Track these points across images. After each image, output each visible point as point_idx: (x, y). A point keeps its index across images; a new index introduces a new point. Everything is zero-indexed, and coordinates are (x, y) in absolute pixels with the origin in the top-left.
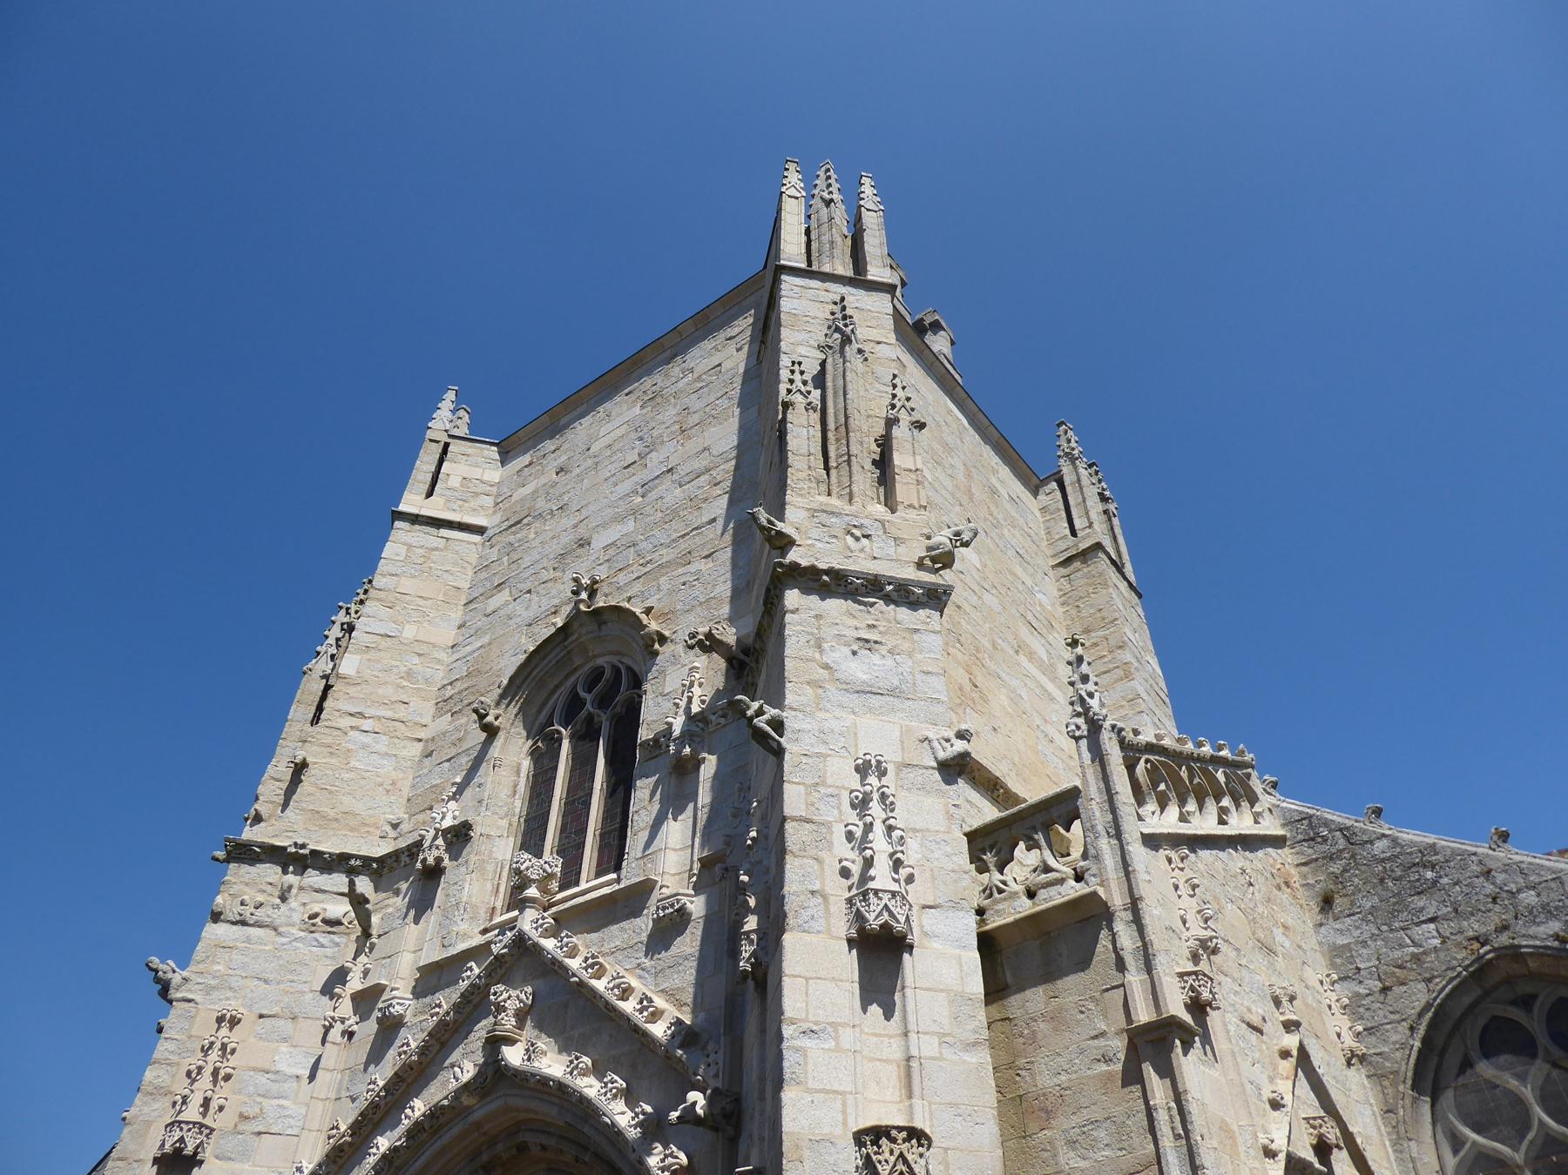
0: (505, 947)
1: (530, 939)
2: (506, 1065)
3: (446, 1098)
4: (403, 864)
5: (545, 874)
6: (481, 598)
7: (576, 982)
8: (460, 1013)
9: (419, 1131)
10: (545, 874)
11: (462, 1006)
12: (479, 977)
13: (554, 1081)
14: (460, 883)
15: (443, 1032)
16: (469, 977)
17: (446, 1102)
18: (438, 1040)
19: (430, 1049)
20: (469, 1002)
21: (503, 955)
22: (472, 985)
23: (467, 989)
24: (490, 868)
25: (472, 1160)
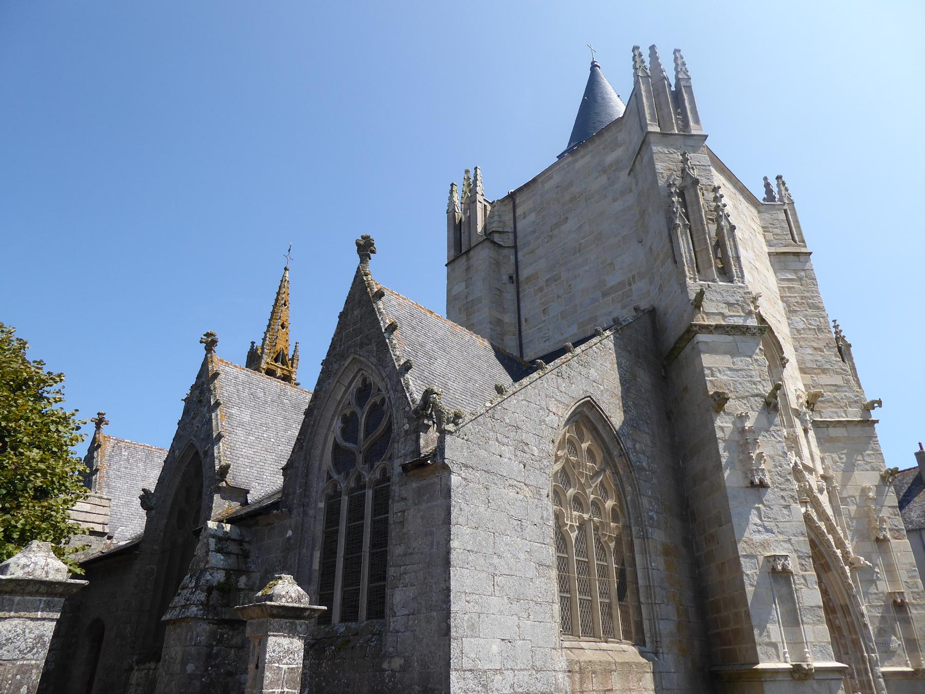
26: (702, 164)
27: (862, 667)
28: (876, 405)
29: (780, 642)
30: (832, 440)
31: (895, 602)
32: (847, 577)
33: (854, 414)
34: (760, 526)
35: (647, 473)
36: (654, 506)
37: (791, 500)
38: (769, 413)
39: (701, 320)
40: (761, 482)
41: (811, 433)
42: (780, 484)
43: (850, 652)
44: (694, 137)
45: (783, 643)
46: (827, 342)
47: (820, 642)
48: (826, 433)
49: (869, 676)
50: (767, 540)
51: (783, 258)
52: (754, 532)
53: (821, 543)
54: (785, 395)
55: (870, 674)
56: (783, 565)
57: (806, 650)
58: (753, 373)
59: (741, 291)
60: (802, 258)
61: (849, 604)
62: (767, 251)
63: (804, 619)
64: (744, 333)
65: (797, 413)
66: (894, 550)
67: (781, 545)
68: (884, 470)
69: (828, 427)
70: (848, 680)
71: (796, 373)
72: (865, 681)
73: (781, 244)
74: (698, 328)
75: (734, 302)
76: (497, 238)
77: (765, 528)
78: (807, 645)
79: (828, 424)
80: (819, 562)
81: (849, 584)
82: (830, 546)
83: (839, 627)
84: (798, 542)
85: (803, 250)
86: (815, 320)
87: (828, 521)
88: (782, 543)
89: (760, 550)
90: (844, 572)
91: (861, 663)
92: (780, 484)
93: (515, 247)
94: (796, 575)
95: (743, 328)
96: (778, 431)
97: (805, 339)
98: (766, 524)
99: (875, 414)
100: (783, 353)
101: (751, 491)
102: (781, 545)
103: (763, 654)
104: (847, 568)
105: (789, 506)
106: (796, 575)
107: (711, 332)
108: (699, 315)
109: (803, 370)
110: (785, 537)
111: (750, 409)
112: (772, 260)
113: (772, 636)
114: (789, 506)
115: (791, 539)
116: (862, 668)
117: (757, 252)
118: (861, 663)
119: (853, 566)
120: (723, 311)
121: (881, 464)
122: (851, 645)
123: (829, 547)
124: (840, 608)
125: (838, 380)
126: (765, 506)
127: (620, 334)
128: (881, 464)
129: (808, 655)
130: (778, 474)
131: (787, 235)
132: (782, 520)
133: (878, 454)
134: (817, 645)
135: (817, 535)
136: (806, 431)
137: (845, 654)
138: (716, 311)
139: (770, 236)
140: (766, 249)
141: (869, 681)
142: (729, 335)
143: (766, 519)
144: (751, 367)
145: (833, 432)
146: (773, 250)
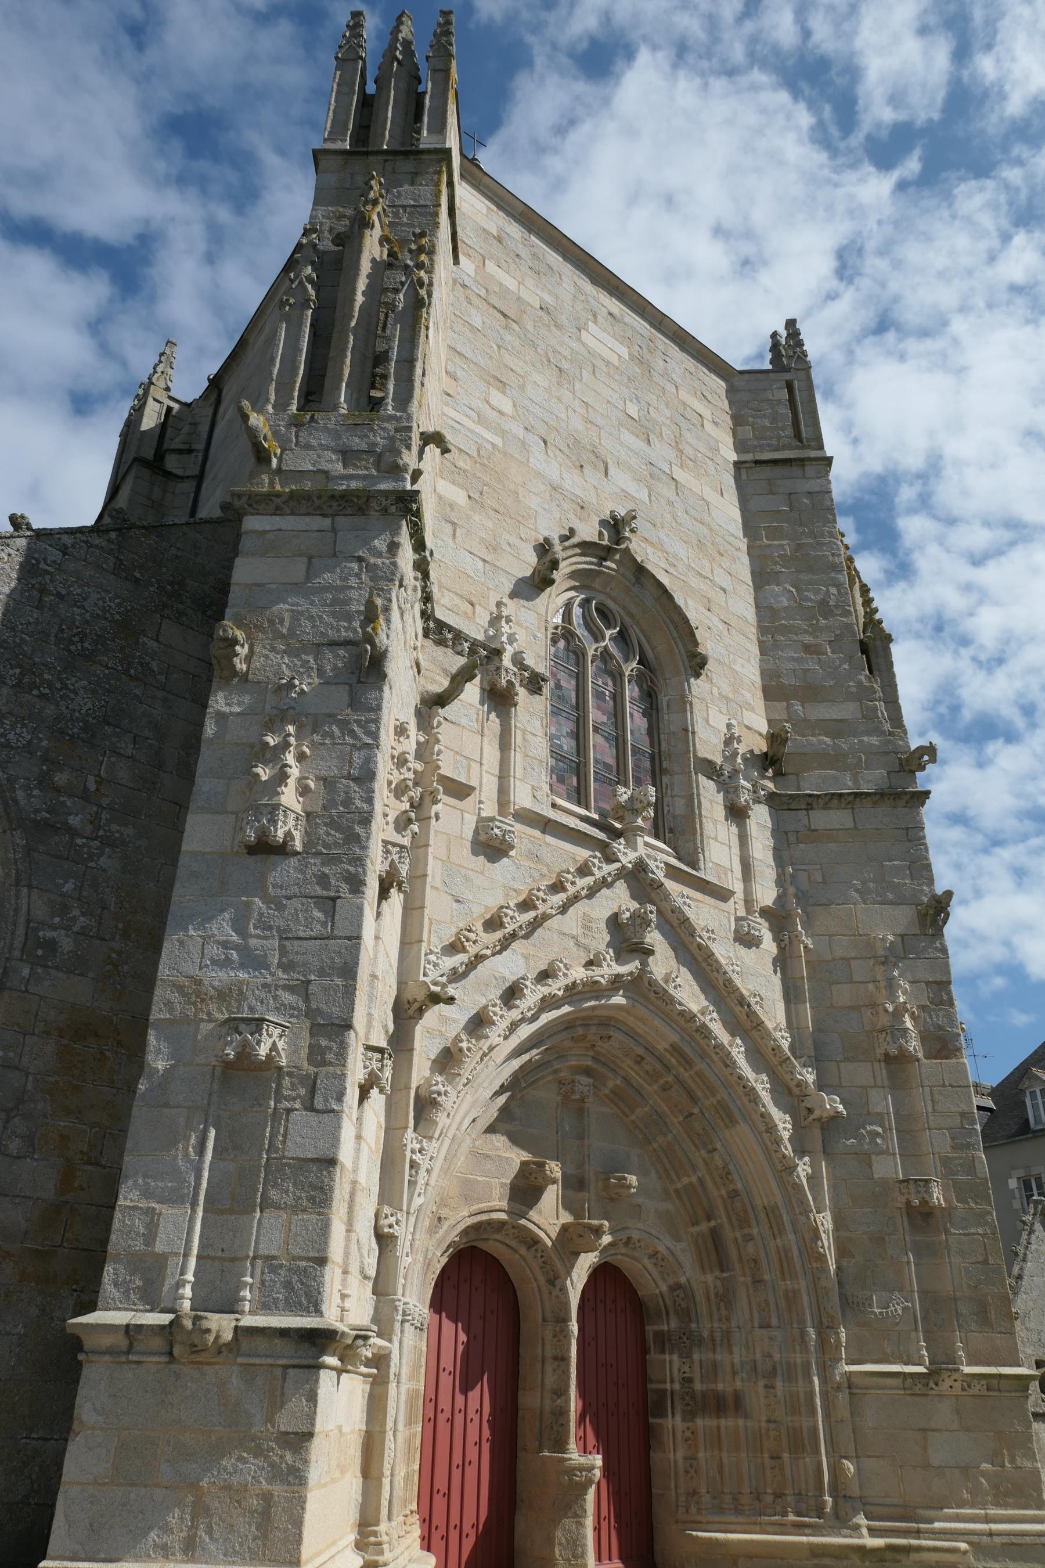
4: (459, 648)
6: (472, 366)
25: (566, 1028)
26: (422, 202)
27: (799, 1359)
28: (926, 758)
29: (177, 1254)
30: (813, 835)
31: (908, 1203)
32: (778, 1141)
33: (871, 780)
34: (236, 947)
35: (79, 841)
36: (74, 919)
37: (344, 887)
38: (359, 682)
39: (264, 483)
40: (263, 836)
41: (760, 817)
42: (326, 846)
43: (774, 1321)
44: (425, 157)
45: (186, 1255)
46: (838, 632)
47: (296, 1258)
48: (805, 821)
49: (812, 1382)
50: (241, 982)
51: (767, 472)
52: (214, 962)
53: (703, 1056)
54: (686, 730)
55: (816, 1379)
56: (245, 1044)
57: (249, 1280)
58: (354, 594)
59: (390, 426)
60: (810, 470)
61: (780, 1203)
62: (733, 457)
63: (274, 1194)
64: (362, 511)
65: (710, 769)
66: (926, 1083)
67: (275, 998)
68: (925, 900)
69: (809, 807)
70: (761, 1390)
71: (748, 695)
72: (802, 1395)
73: (769, 445)
74: (244, 499)
75: (365, 447)
76: (172, 463)
77: (244, 950)
78: (253, 1265)
79: (810, 802)
80: (707, 1103)
81: (784, 1156)
82: (728, 1062)
83: (755, 1261)
84: (326, 990)
85: (813, 454)
86: (817, 592)
87: (743, 1007)
88: (280, 992)
89: (213, 1007)
90: (771, 1128)
91: (797, 1348)
92: (326, 846)
93: (200, 478)
94: (290, 1074)
95: (359, 497)
96: (368, 721)
97: (785, 630)
98: (253, 942)
99: (922, 780)
100: (696, 644)
101: (250, 860)
102: (275, 998)
103: (116, 1285)
104: (783, 1123)
105: (334, 899)
106: (290, 1074)
107: (278, 511)
108: (265, 478)
109: (772, 691)
110: (295, 976)
111: (314, 674)
112: (744, 476)
113: (161, 1235)
114: (334, 899)
115: (309, 982)
116: (799, 1361)
117: (689, 451)
118: (797, 1348)
119: (812, 1117)
120: (324, 466)
121: (925, 888)
122: (783, 1304)
123: (727, 1066)
124: (762, 1215)
125: (847, 711)
126: (267, 899)
127: (109, 541)
128: (925, 888)
129: (246, 1293)
130: (333, 820)
131: (783, 429)
132: (301, 934)
133: (922, 869)
134: (281, 1266)
135: (691, 1036)
136: (737, 813)
137: (761, 1327)
138: (312, 468)
139: (747, 432)
140: (733, 457)
141: (811, 1394)
142: (324, 515)
143: (258, 932)
144: (353, 582)
145: (821, 819)
146: (749, 457)
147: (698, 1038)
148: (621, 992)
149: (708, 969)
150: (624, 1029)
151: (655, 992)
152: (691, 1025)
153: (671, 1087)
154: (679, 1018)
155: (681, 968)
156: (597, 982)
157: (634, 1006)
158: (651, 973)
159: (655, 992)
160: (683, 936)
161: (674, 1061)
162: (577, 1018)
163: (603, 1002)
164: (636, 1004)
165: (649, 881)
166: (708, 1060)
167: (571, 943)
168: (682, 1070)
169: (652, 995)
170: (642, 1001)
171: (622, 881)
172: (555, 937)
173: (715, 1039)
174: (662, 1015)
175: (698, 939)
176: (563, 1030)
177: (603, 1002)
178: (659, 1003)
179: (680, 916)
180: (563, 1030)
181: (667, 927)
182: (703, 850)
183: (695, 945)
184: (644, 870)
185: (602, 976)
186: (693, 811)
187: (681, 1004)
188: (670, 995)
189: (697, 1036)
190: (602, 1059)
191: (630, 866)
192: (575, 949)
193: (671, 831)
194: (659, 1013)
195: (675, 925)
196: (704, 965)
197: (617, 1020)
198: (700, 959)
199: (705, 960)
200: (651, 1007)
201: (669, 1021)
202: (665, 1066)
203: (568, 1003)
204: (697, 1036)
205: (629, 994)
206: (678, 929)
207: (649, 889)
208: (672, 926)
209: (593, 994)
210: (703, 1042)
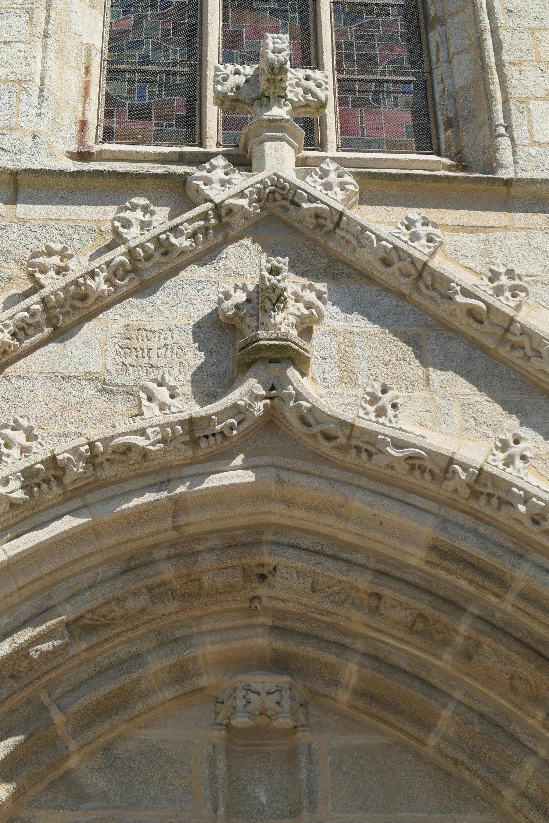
0: (241, 194)
1: (312, 199)
2: (312, 409)
3: (142, 432)
5: (309, 97)
7: (471, 312)
8: (112, 285)
9: (47, 481)
10: (309, 97)
11: (120, 273)
12: (174, 230)
13: (465, 468)
14: (23, 46)
15: (67, 308)
16: (144, 225)
17: (140, 441)
18: (51, 321)
19: (31, 331)
20: (135, 271)
21: (230, 211)
22: (156, 239)
23: (142, 246)
24: (71, 44)
147: (487, 510)
148: (238, 460)
149: (515, 356)
150: (306, 544)
151: (328, 437)
152: (450, 485)
153: (479, 645)
154: (416, 479)
155: (434, 373)
156: (129, 448)
157: (280, 482)
158: (299, 396)
159: (328, 437)
160: (431, 306)
161: (463, 583)
162: (155, 546)
163: (182, 489)
164: (285, 476)
165: (311, 222)
166: (536, 557)
167: (90, 390)
168: (493, 599)
169: (325, 446)
170: (306, 466)
171: (247, 241)
172: (41, 390)
173: (526, 499)
174: (373, 486)
175: (460, 299)
176: (114, 578)
177: (182, 489)
178: (351, 457)
179: (406, 265)
180: (114, 578)
181: (389, 300)
182: (508, 128)
183: (461, 315)
184: (293, 202)
185: (142, 432)
186: (484, 66)
187: (398, 444)
188: (364, 431)
189: (481, 505)
190: (299, 626)
191: (244, 202)
192: (100, 402)
193: (450, 123)
194: (363, 482)
195: (406, 290)
196: (504, 352)
197: (279, 529)
198: (488, 342)
199: (503, 340)
200: (335, 474)
201: (397, 493)
202: (446, 600)
203: (70, 513)
204: (481, 505)
205: (264, 460)
206: (416, 297)
207: (319, 237)
208: (402, 296)
209: (150, 480)
210: (502, 516)
